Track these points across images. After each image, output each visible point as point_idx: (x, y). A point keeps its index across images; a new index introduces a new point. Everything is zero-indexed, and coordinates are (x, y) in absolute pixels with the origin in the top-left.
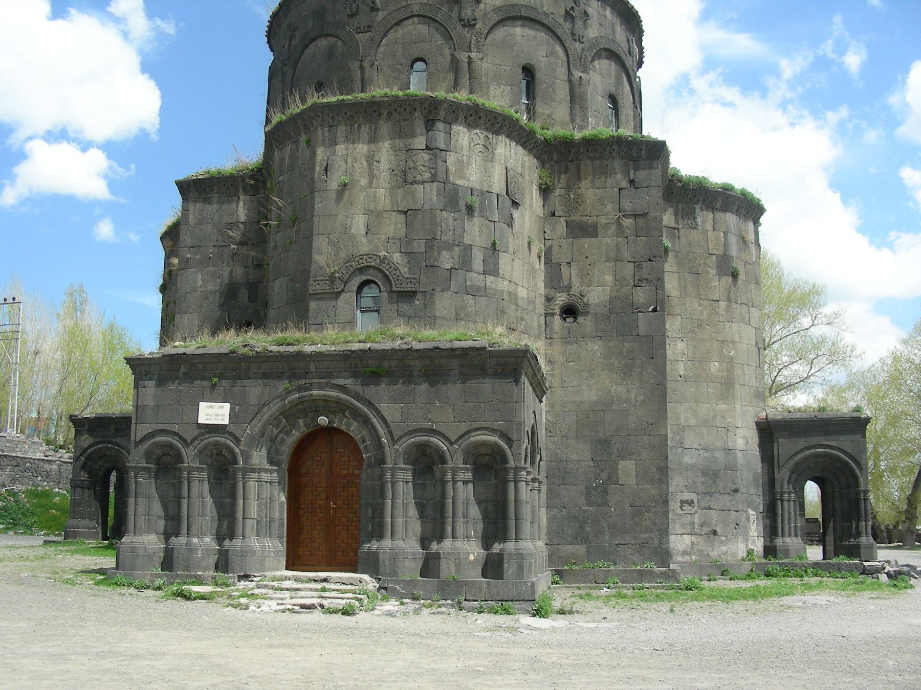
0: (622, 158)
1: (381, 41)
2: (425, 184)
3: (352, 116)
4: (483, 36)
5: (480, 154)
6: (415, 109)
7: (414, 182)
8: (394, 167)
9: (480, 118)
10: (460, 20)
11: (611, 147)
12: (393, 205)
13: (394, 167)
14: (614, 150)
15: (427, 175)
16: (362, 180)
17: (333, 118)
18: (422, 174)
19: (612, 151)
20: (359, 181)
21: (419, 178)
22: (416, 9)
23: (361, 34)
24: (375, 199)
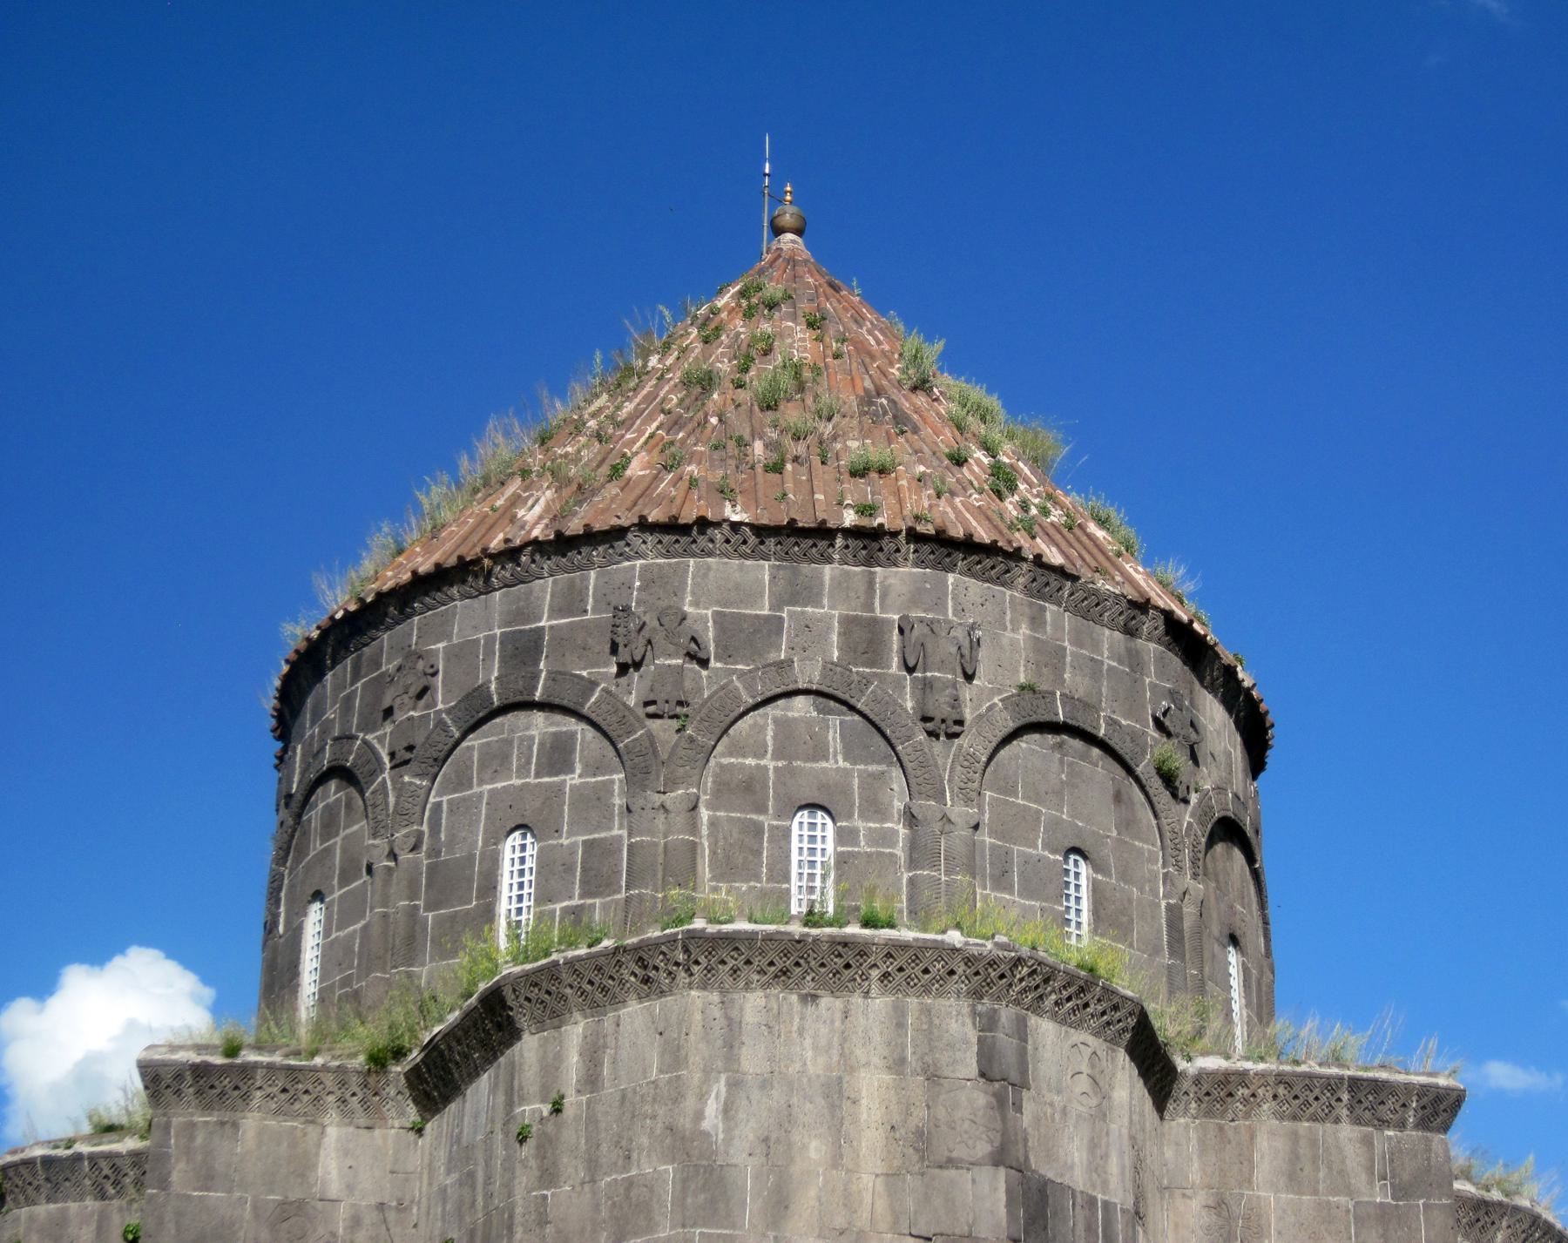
0: (1358, 1121)
1: (714, 747)
2: (976, 1169)
3: (785, 972)
4: (980, 767)
5: (1084, 1099)
6: (952, 973)
7: (951, 1163)
8: (896, 1119)
9: (1086, 1005)
10: (926, 719)
11: (1333, 1092)
12: (896, 1221)
13: (896, 1119)
14: (1339, 1100)
15: (983, 1149)
16: (814, 1144)
17: (735, 971)
18: (970, 1142)
19: (1333, 1103)
20: (805, 1147)
21: (960, 1152)
22: (808, 673)
23: (658, 722)
24: (849, 1201)
